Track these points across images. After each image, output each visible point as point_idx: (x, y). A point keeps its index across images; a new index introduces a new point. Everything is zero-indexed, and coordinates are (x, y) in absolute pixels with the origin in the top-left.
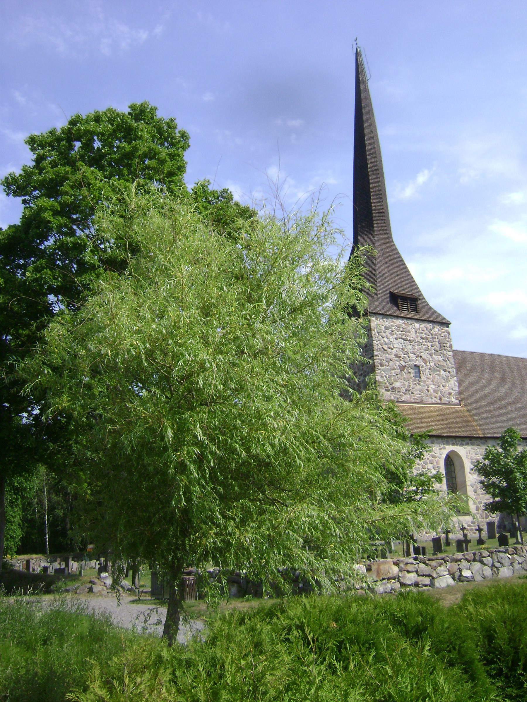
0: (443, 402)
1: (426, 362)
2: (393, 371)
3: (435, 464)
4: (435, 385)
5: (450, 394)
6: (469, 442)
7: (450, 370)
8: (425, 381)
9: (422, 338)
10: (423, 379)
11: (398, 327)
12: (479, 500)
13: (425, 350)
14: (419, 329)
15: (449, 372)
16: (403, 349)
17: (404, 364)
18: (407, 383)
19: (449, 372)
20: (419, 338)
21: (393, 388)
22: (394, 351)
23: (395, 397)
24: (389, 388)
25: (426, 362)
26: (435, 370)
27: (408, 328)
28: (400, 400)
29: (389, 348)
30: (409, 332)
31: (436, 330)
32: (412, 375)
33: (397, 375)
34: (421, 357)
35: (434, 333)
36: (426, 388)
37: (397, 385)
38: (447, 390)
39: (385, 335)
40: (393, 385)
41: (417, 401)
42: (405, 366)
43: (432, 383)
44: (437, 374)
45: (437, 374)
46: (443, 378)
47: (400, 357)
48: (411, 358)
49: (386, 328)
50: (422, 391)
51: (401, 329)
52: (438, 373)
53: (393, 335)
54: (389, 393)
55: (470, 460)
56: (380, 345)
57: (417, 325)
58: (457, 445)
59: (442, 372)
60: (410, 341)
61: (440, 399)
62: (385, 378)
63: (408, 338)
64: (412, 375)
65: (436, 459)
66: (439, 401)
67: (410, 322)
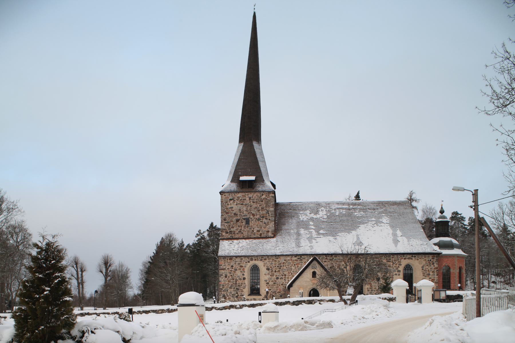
0: (262, 236)
1: (253, 215)
2: (232, 223)
3: (242, 270)
4: (259, 227)
5: (268, 232)
6: (267, 258)
7: (270, 218)
8: (252, 226)
9: (253, 202)
10: (250, 225)
11: (238, 198)
12: (270, 288)
13: (255, 209)
14: (252, 197)
15: (269, 219)
16: (240, 210)
17: (239, 218)
18: (240, 228)
19: (269, 219)
20: (252, 203)
21: (230, 232)
22: (234, 212)
23: (231, 236)
24: (228, 232)
25: (253, 215)
26: (259, 220)
27: (245, 198)
28: (234, 237)
29: (231, 210)
30: (245, 200)
31: (264, 196)
32: (244, 223)
33: (234, 224)
34: (251, 213)
35: (262, 198)
36: (252, 229)
37: (232, 230)
38: (266, 229)
39: (229, 203)
40: (231, 230)
41: (245, 237)
42: (240, 219)
43: (257, 227)
44: (260, 222)
45: (260, 222)
46: (265, 223)
47: (237, 214)
48: (244, 214)
49: (230, 200)
50: (249, 231)
51: (240, 199)
52: (262, 220)
53: (235, 202)
54: (228, 234)
55: (266, 268)
56: (226, 210)
57: (250, 195)
58: (258, 260)
59: (264, 220)
60: (246, 205)
61: (261, 235)
62: (226, 227)
63: (244, 203)
64: (244, 223)
65: (243, 268)
66: (259, 236)
67: (247, 193)
